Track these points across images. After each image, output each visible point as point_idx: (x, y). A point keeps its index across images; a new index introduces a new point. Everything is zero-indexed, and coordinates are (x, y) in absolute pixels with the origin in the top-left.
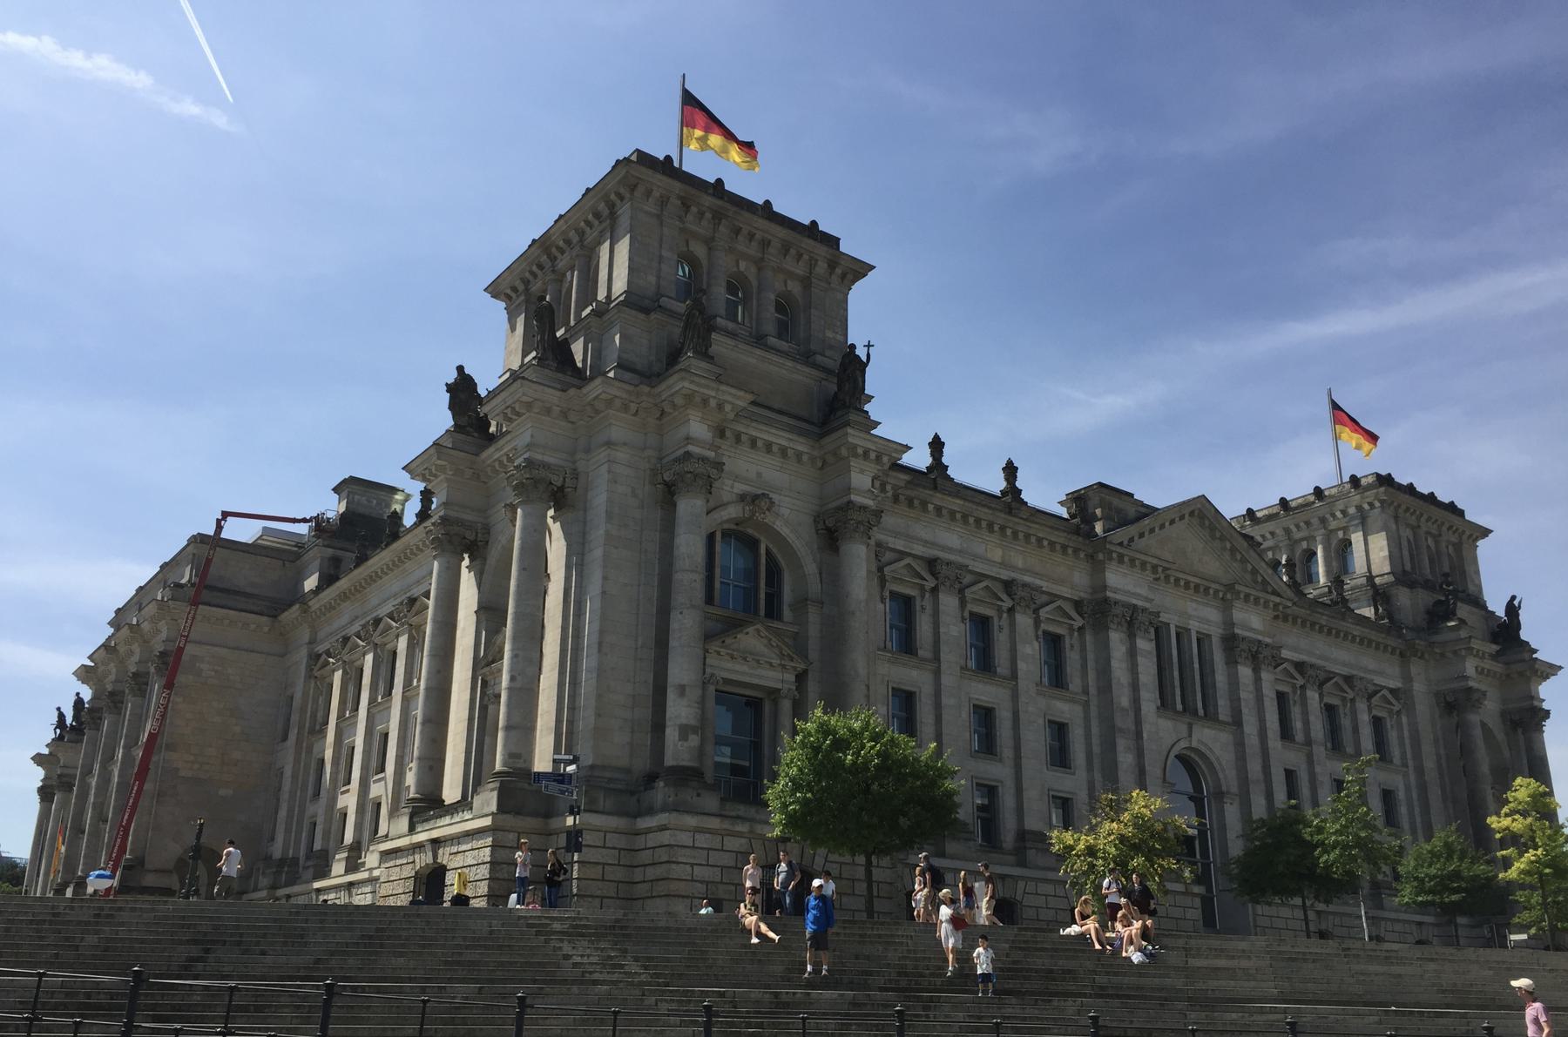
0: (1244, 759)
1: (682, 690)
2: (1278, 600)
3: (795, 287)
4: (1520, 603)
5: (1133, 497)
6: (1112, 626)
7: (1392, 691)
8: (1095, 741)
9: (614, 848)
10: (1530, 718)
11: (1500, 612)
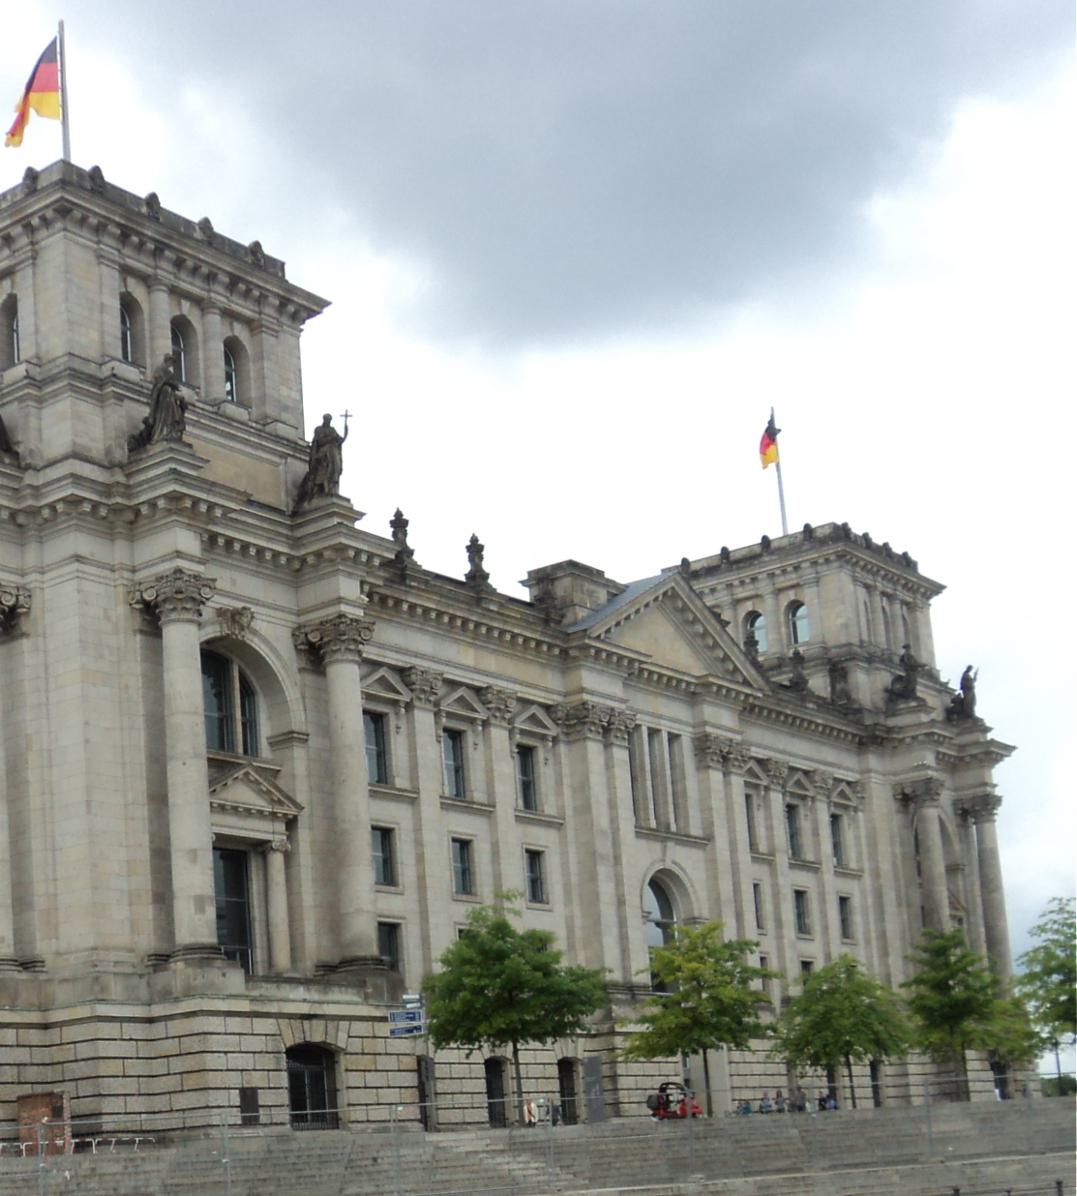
0: (715, 878)
1: (193, 855)
2: (748, 691)
3: (240, 331)
4: (976, 674)
5: (603, 575)
6: (589, 735)
7: (849, 783)
8: (574, 868)
9: (131, 1039)
10: (978, 808)
11: (955, 685)
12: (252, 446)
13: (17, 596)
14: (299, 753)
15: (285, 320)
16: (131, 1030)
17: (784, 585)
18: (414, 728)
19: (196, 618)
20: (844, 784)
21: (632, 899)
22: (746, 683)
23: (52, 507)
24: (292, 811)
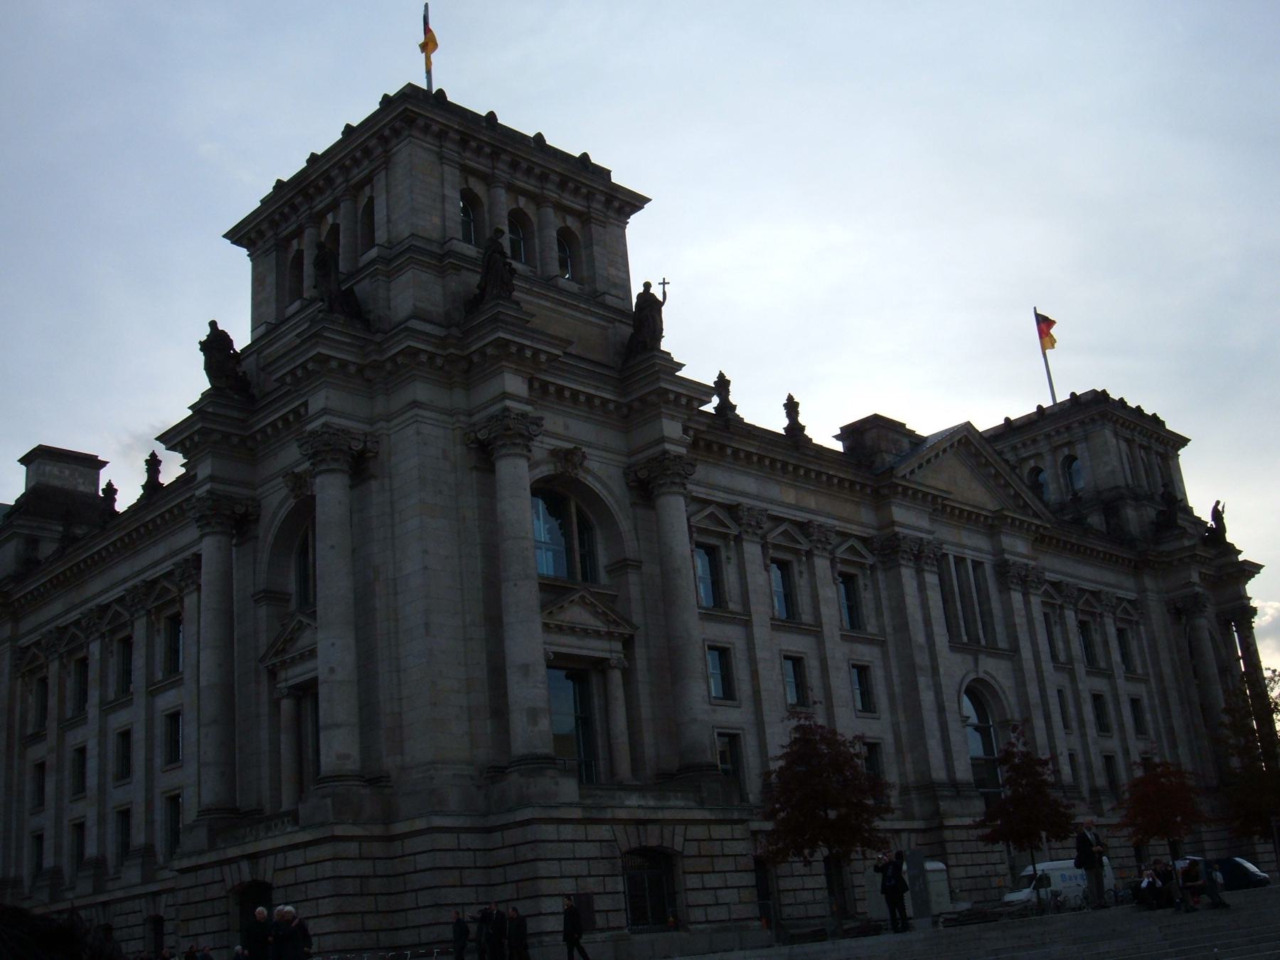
3: (571, 222)
4: (1223, 507)
6: (903, 562)
7: (1129, 601)
8: (896, 681)
9: (469, 849)
12: (581, 312)
13: (365, 442)
14: (633, 578)
15: (611, 213)
16: (469, 840)
17: (1058, 443)
18: (743, 557)
19: (525, 452)
20: (1125, 602)
21: (950, 705)
22: (1036, 515)
23: (393, 359)
24: (627, 631)
